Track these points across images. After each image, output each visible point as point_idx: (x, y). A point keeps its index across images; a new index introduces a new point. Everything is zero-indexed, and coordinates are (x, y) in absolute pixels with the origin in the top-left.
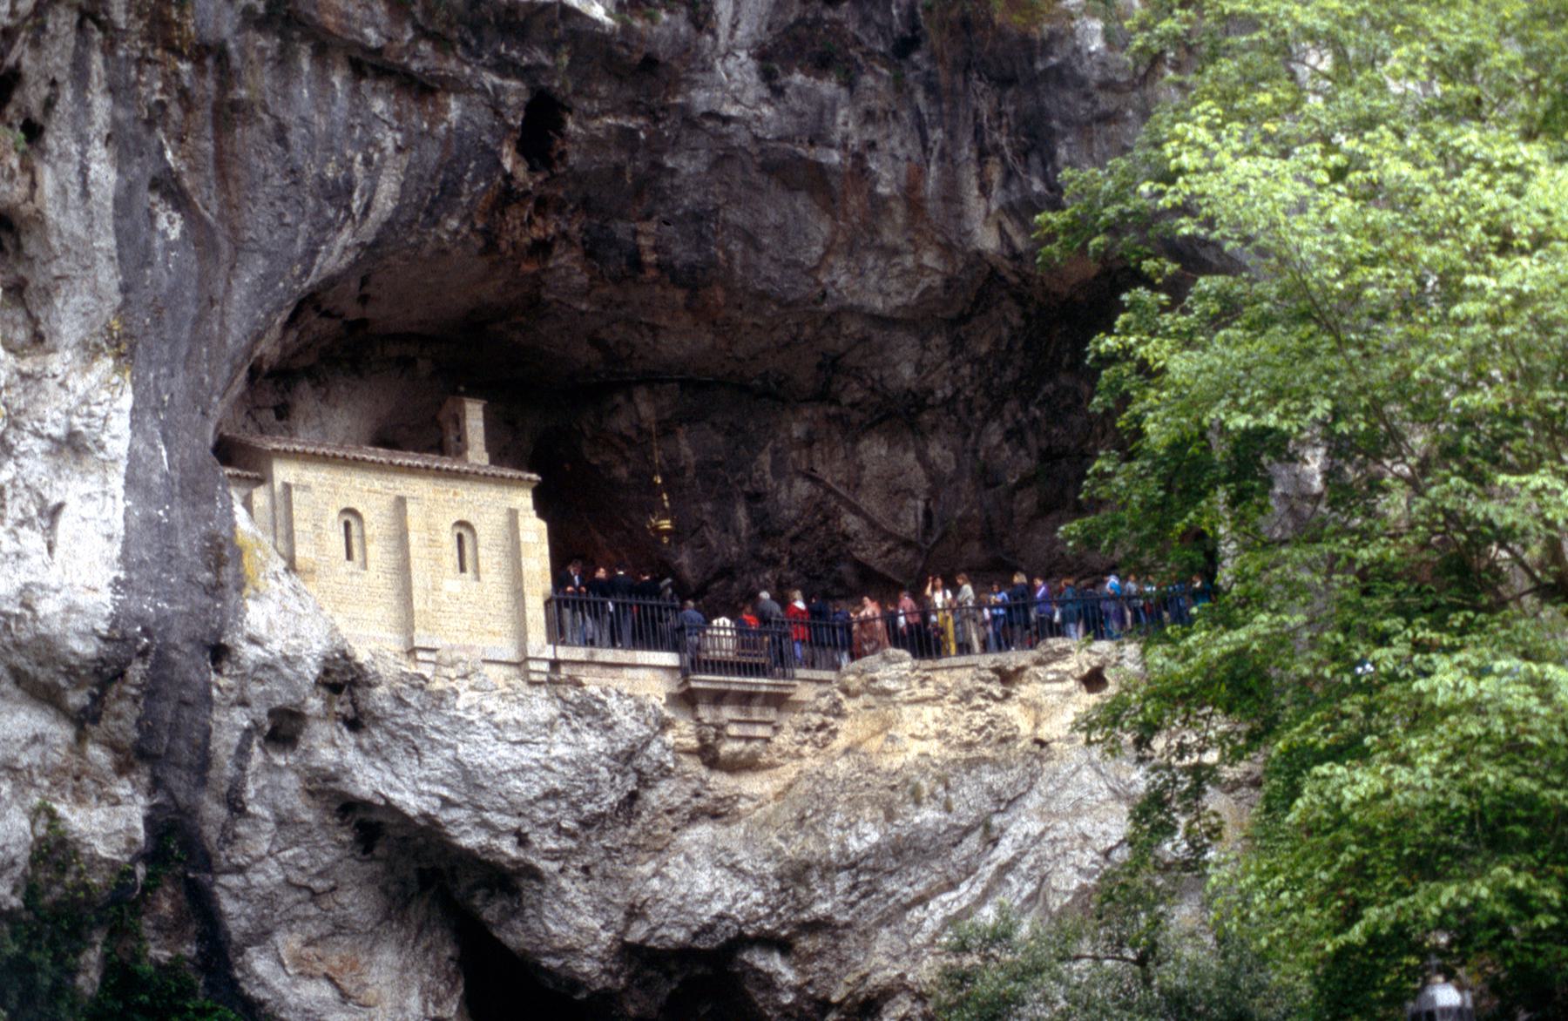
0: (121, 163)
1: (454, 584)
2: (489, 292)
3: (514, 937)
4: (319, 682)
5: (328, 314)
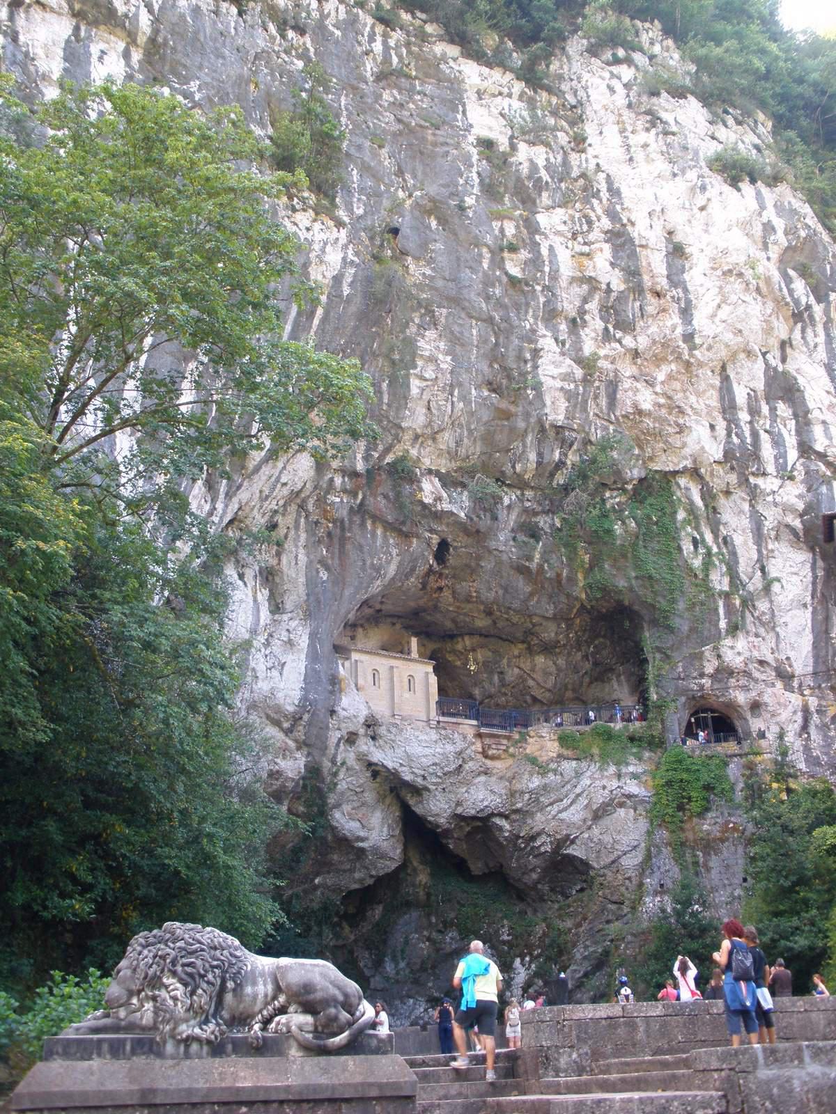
0: (308, 555)
1: (407, 695)
2: (421, 602)
3: (418, 810)
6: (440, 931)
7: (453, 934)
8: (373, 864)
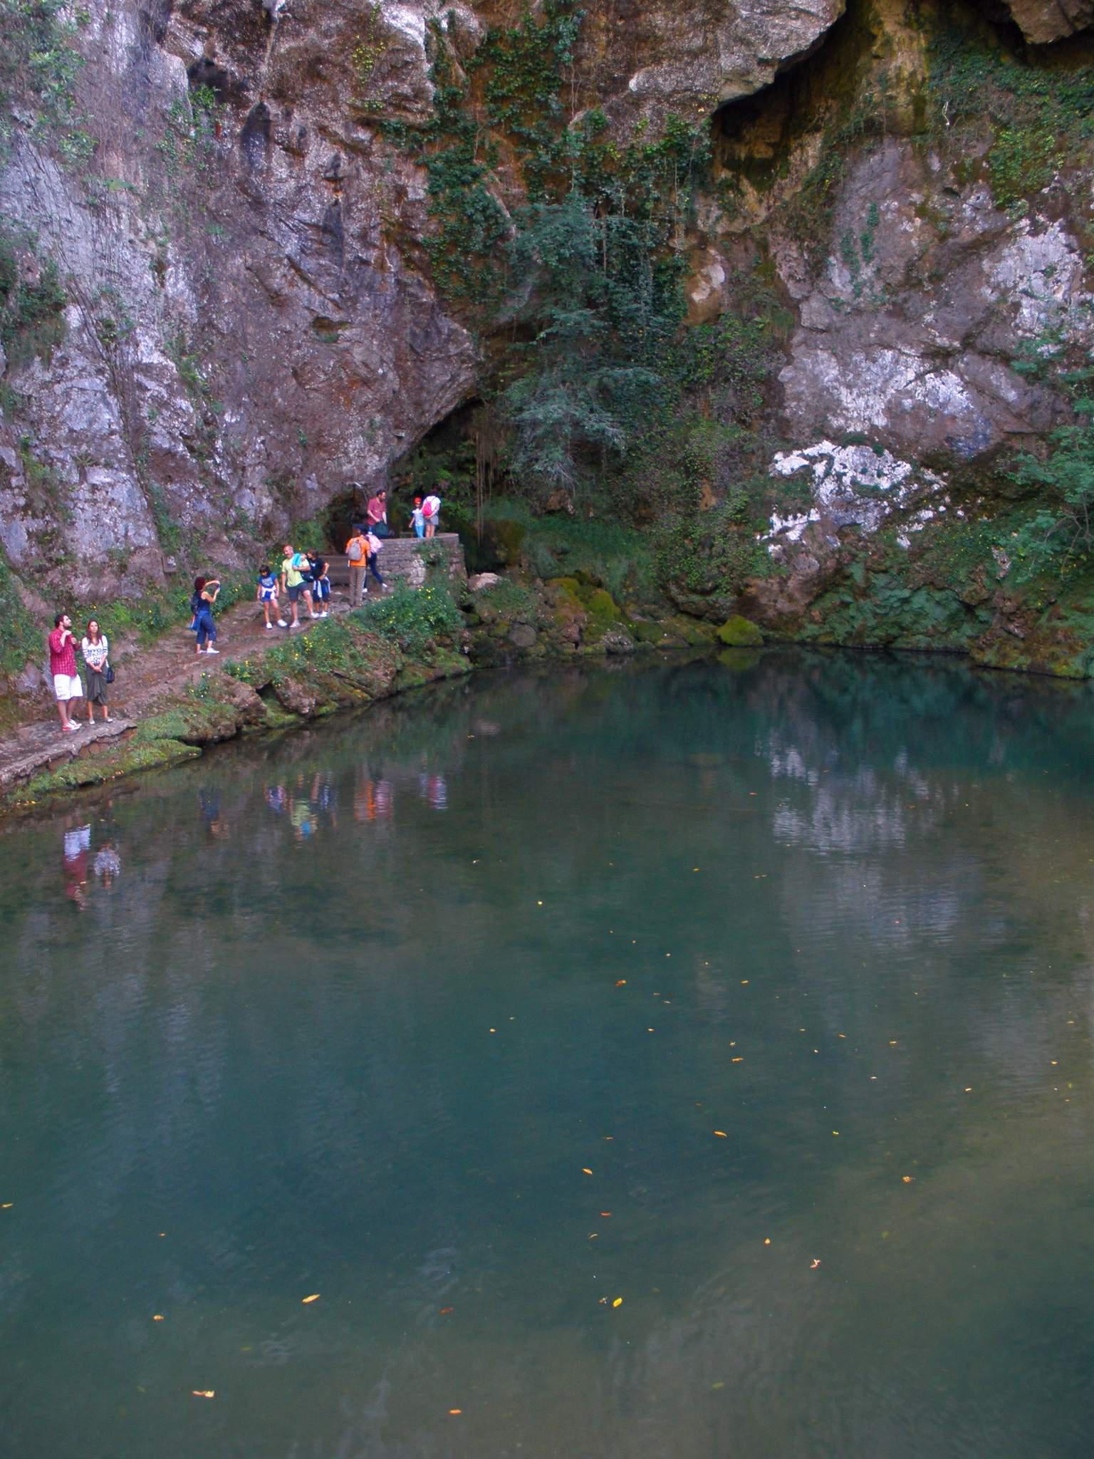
6: (948, 191)
7: (977, 197)
8: (757, 29)
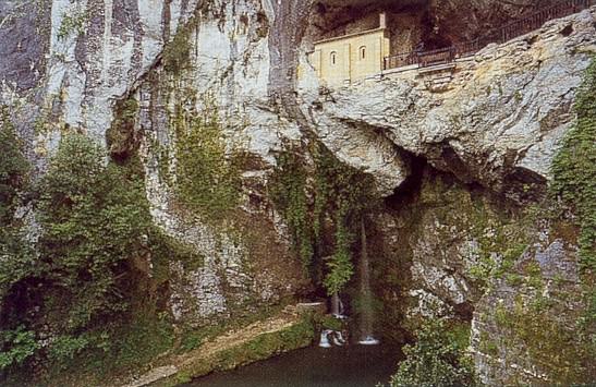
3: (398, 143)
4: (321, 94)
5: (335, 7)
